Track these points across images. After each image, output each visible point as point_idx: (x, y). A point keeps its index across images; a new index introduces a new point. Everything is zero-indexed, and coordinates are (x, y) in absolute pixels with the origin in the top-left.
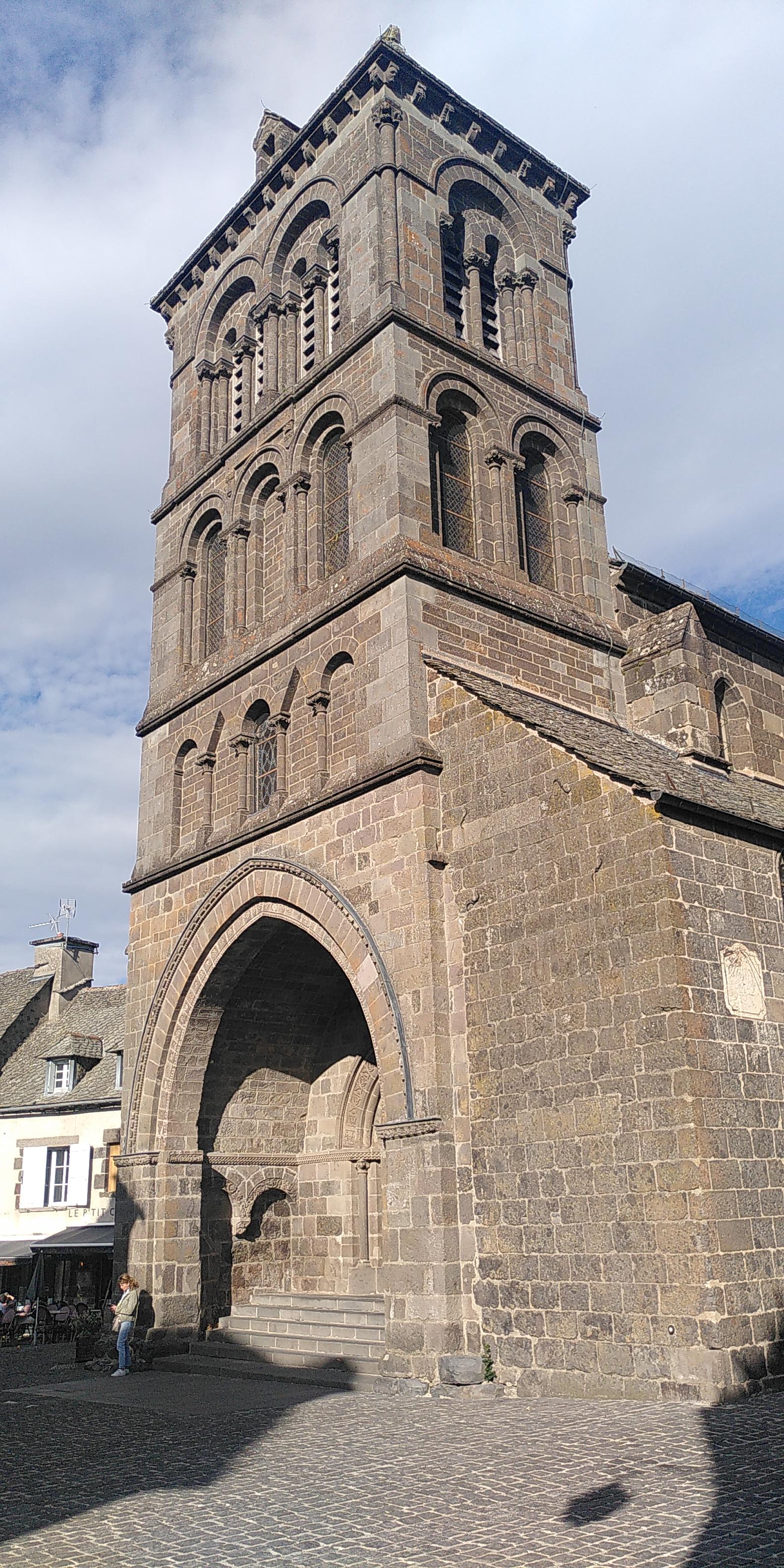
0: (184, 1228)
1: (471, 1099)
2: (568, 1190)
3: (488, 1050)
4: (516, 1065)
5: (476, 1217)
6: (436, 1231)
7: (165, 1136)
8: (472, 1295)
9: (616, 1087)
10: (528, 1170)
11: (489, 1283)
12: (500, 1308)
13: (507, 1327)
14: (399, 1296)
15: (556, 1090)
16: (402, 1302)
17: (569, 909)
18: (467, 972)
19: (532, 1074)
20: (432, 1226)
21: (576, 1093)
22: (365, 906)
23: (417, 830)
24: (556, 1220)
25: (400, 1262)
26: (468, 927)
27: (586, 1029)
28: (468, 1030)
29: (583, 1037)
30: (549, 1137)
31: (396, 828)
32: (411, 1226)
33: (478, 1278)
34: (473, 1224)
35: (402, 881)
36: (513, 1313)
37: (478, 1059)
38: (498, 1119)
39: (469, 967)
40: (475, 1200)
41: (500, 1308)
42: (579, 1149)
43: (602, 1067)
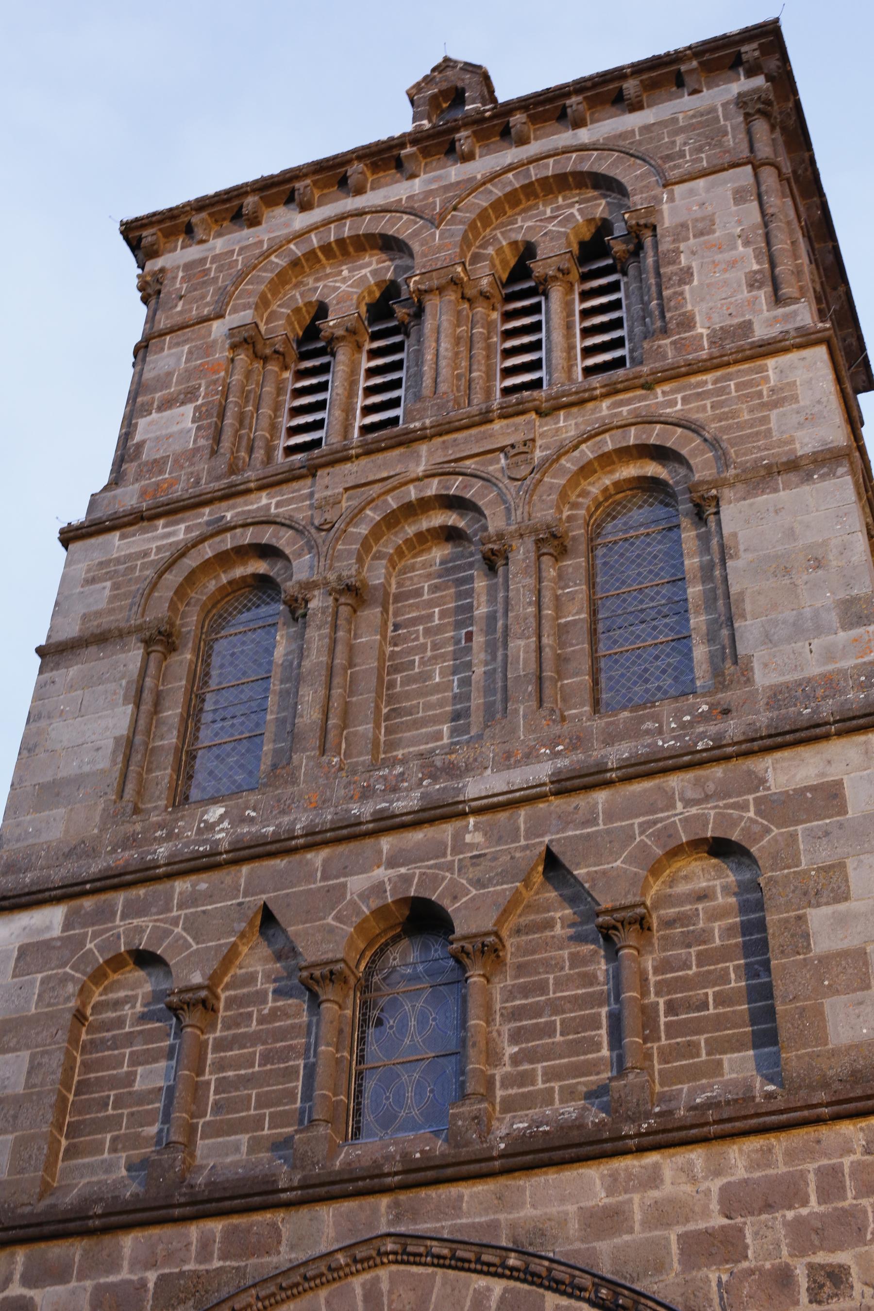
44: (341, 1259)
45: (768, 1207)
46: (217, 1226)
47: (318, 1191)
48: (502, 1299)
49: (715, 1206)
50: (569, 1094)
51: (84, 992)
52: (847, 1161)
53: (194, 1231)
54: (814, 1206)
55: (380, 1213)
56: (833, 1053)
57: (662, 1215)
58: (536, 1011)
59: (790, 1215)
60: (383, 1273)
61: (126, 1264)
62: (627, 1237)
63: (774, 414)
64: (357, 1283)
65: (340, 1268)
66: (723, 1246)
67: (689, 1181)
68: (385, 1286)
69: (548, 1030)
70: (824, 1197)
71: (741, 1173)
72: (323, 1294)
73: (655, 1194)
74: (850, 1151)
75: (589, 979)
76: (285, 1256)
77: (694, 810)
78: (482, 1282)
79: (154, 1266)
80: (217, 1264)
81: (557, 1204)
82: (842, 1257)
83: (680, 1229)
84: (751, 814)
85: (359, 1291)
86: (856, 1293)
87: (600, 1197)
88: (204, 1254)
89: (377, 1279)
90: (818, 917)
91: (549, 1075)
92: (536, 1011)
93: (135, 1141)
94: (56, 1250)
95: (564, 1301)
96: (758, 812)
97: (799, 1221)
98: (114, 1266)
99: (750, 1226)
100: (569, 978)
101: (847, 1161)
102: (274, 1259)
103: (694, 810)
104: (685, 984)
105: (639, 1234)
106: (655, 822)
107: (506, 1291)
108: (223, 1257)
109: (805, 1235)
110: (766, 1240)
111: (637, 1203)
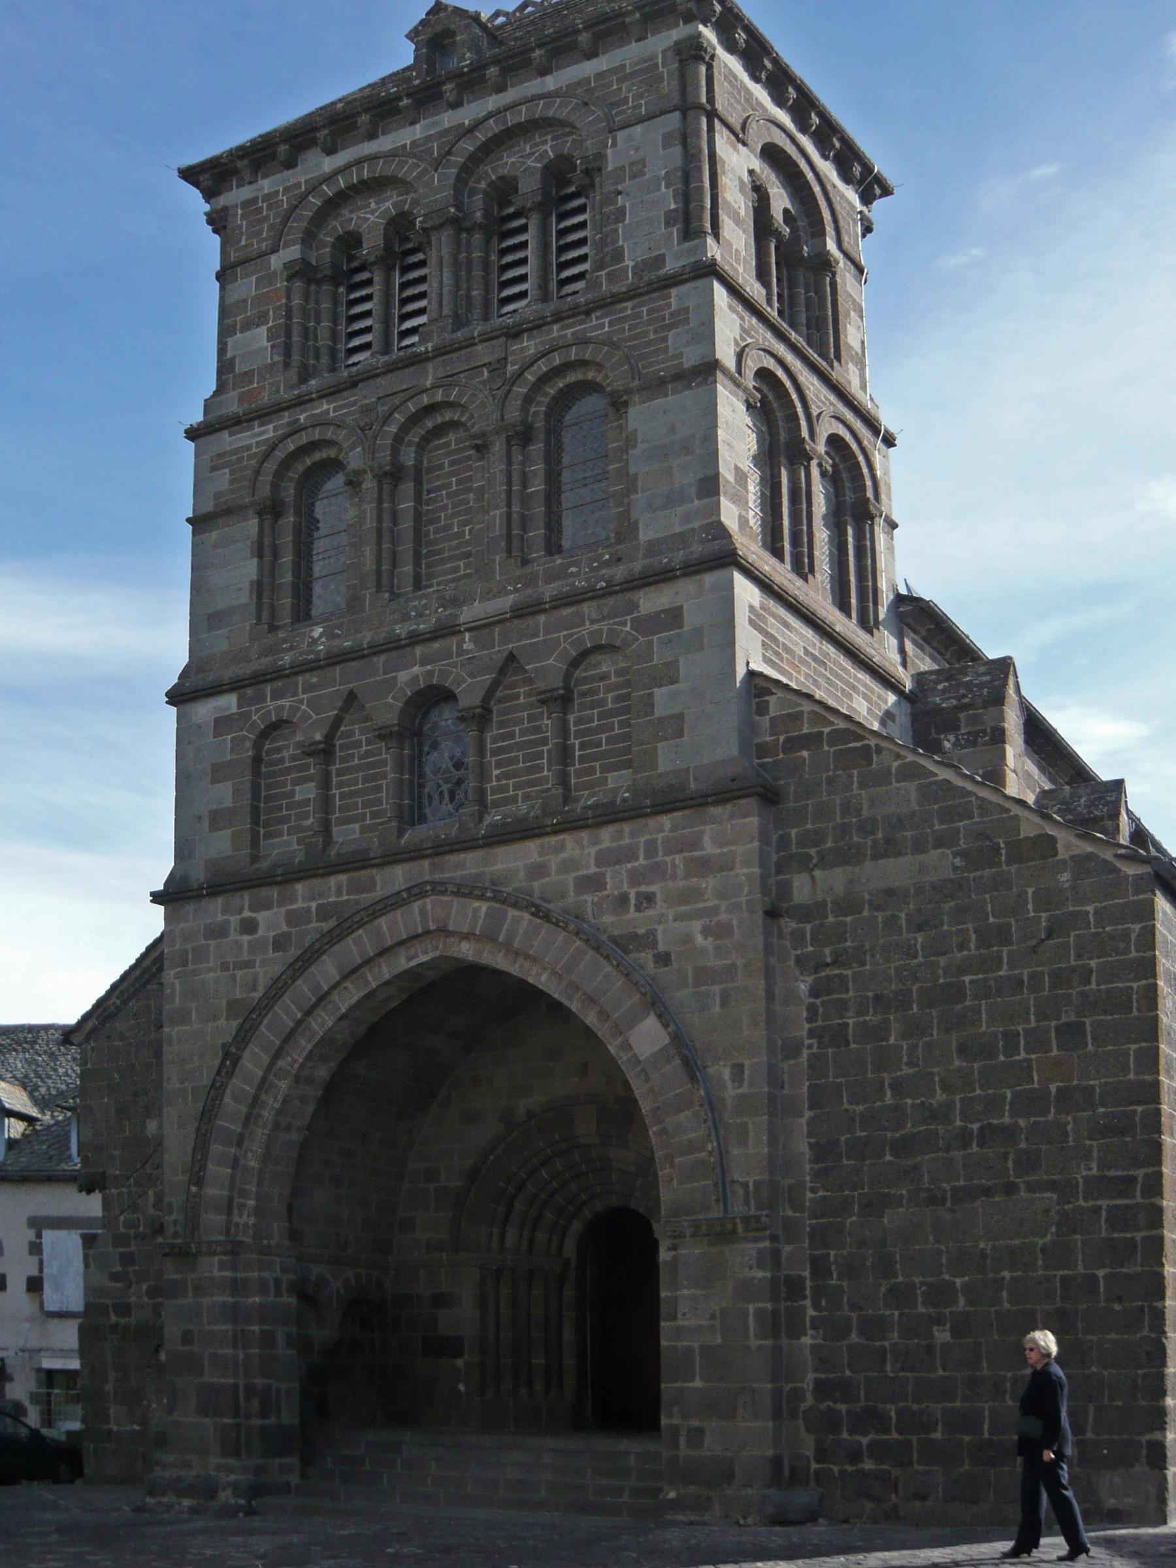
0: (281, 1338)
1: (809, 1195)
2: (962, 1302)
3: (843, 1138)
4: (888, 1158)
5: (810, 1332)
6: (760, 1347)
7: (252, 1221)
8: (801, 1423)
9: (1052, 1186)
10: (900, 1279)
11: (828, 1407)
12: (845, 1435)
13: (855, 1455)
14: (695, 1423)
15: (954, 1189)
16: (700, 1431)
17: (992, 982)
18: (810, 1047)
19: (915, 1168)
20: (754, 1343)
21: (988, 1192)
23: (746, 872)
24: (942, 1335)
25: (698, 1383)
26: (815, 992)
27: (1007, 1120)
28: (808, 1114)
29: (1002, 1129)
30: (937, 1241)
32: (719, 1341)
33: (810, 1400)
34: (806, 1340)
35: (719, 931)
36: (865, 1441)
37: (823, 1151)
38: (854, 1218)
39: (814, 1041)
40: (811, 1312)
41: (845, 1435)
42: (983, 1254)
43: (1028, 1162)
44: (405, 895)
45: (618, 861)
46: (343, 878)
48: (487, 913)
49: (592, 862)
50: (527, 797)
52: (660, 836)
53: (332, 881)
54: (642, 861)
55: (424, 869)
56: (660, 775)
58: (509, 749)
59: (629, 866)
60: (428, 901)
61: (300, 899)
62: (547, 879)
64: (416, 906)
65: (404, 899)
67: (581, 849)
68: (429, 907)
69: (515, 760)
70: (647, 857)
71: (606, 844)
72: (399, 912)
73: (563, 855)
74: (662, 831)
75: (538, 730)
76: (379, 893)
77: (596, 627)
78: (476, 904)
79: (313, 899)
80: (345, 897)
82: (654, 888)
83: (574, 874)
84: (628, 629)
85: (417, 910)
86: (657, 907)
88: (339, 893)
89: (425, 903)
91: (517, 787)
92: (509, 749)
93: (300, 829)
94: (264, 892)
95: (517, 913)
96: (632, 628)
97: (634, 869)
98: (293, 900)
99: (609, 872)
100: (527, 729)
101: (660, 836)
102: (373, 895)
103: (596, 627)
104: (589, 732)
105: (554, 877)
106: (572, 635)
107: (489, 908)
108: (348, 894)
109: (636, 878)
110: (616, 880)
111: (554, 861)
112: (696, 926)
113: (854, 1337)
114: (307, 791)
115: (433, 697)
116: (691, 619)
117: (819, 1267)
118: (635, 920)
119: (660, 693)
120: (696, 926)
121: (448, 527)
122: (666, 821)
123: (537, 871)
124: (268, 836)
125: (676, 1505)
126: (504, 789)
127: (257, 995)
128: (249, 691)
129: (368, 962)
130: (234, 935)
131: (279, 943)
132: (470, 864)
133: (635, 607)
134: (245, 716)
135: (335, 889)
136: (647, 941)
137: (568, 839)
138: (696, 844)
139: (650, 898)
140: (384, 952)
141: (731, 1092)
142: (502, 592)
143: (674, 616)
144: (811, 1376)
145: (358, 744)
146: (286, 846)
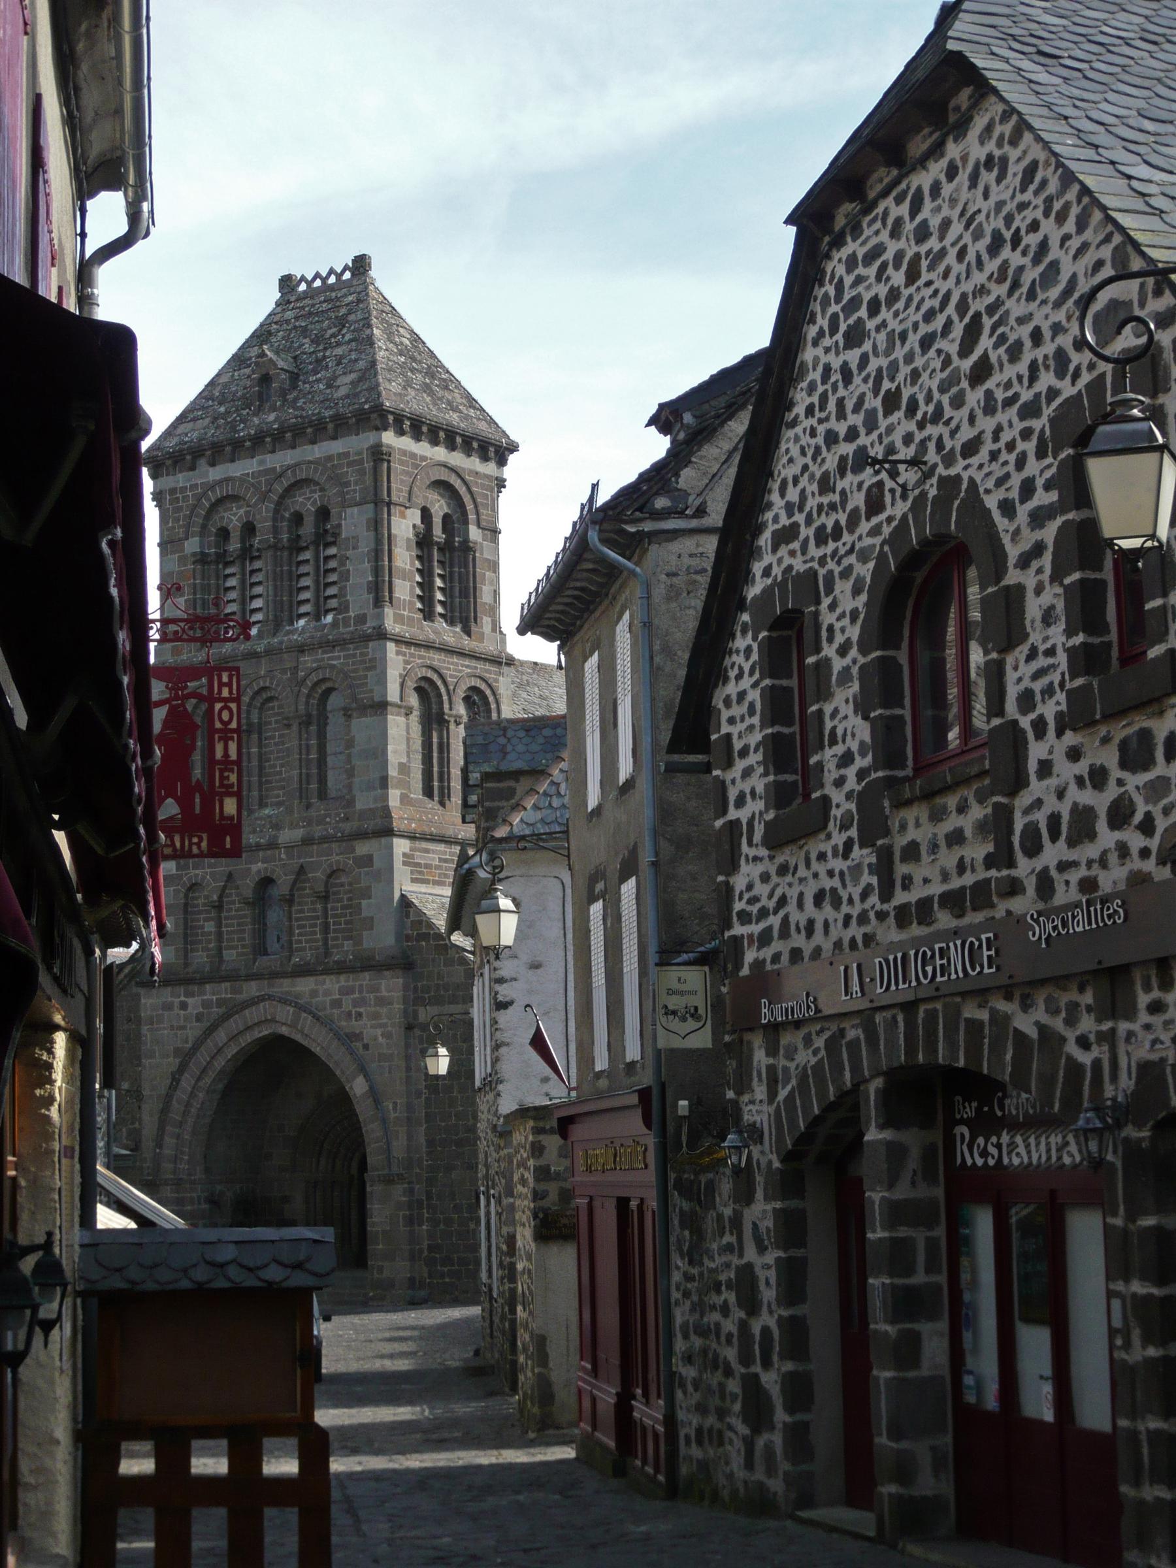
13: (442, 1276)
22: (359, 1045)
31: (381, 1002)
37: (431, 1143)
47: (250, 977)
51: (186, 896)
57: (327, 993)
63: (370, 674)
66: (337, 1004)
67: (332, 985)
69: (304, 926)
75: (314, 910)
81: (304, 986)
87: (313, 986)
90: (364, 903)
93: (208, 949)
94: (190, 987)
109: (356, 1003)
112: (379, 1032)
113: (442, 1227)
114: (210, 927)
115: (266, 882)
116: (377, 863)
117: (429, 1196)
118: (355, 1025)
119: (364, 903)
120: (379, 1032)
121: (274, 766)
122: (367, 975)
123: (314, 993)
124: (192, 950)
125: (372, 1299)
126: (300, 942)
127: (189, 1045)
128: (182, 862)
129: (240, 1033)
130: (176, 1011)
131: (199, 1017)
132: (285, 986)
133: (353, 851)
134: (180, 877)
135: (224, 991)
136: (358, 1037)
137: (328, 978)
138: (378, 990)
139: (359, 1015)
140: (248, 1028)
141: (393, 1115)
142: (297, 827)
143: (370, 858)
144: (426, 1243)
145: (233, 902)
146: (201, 958)
